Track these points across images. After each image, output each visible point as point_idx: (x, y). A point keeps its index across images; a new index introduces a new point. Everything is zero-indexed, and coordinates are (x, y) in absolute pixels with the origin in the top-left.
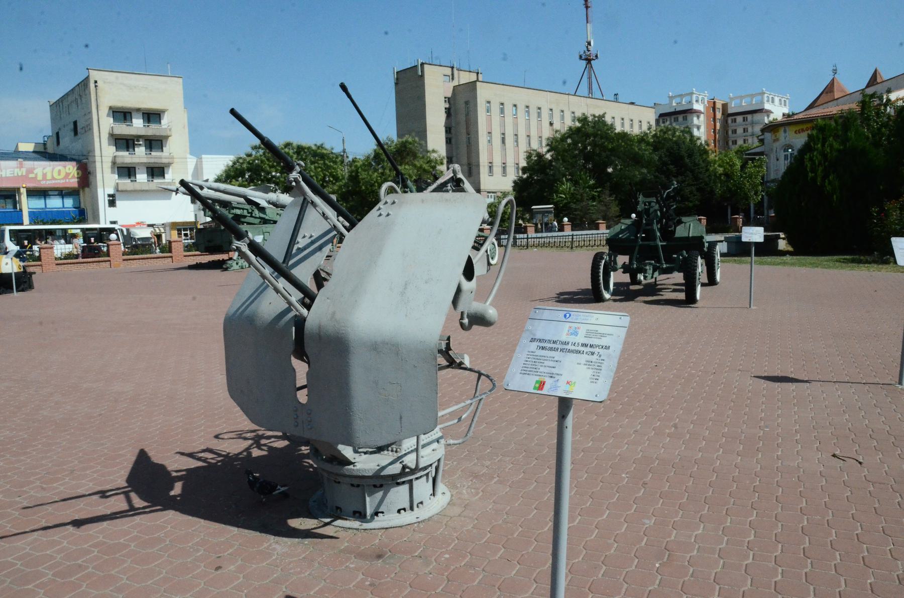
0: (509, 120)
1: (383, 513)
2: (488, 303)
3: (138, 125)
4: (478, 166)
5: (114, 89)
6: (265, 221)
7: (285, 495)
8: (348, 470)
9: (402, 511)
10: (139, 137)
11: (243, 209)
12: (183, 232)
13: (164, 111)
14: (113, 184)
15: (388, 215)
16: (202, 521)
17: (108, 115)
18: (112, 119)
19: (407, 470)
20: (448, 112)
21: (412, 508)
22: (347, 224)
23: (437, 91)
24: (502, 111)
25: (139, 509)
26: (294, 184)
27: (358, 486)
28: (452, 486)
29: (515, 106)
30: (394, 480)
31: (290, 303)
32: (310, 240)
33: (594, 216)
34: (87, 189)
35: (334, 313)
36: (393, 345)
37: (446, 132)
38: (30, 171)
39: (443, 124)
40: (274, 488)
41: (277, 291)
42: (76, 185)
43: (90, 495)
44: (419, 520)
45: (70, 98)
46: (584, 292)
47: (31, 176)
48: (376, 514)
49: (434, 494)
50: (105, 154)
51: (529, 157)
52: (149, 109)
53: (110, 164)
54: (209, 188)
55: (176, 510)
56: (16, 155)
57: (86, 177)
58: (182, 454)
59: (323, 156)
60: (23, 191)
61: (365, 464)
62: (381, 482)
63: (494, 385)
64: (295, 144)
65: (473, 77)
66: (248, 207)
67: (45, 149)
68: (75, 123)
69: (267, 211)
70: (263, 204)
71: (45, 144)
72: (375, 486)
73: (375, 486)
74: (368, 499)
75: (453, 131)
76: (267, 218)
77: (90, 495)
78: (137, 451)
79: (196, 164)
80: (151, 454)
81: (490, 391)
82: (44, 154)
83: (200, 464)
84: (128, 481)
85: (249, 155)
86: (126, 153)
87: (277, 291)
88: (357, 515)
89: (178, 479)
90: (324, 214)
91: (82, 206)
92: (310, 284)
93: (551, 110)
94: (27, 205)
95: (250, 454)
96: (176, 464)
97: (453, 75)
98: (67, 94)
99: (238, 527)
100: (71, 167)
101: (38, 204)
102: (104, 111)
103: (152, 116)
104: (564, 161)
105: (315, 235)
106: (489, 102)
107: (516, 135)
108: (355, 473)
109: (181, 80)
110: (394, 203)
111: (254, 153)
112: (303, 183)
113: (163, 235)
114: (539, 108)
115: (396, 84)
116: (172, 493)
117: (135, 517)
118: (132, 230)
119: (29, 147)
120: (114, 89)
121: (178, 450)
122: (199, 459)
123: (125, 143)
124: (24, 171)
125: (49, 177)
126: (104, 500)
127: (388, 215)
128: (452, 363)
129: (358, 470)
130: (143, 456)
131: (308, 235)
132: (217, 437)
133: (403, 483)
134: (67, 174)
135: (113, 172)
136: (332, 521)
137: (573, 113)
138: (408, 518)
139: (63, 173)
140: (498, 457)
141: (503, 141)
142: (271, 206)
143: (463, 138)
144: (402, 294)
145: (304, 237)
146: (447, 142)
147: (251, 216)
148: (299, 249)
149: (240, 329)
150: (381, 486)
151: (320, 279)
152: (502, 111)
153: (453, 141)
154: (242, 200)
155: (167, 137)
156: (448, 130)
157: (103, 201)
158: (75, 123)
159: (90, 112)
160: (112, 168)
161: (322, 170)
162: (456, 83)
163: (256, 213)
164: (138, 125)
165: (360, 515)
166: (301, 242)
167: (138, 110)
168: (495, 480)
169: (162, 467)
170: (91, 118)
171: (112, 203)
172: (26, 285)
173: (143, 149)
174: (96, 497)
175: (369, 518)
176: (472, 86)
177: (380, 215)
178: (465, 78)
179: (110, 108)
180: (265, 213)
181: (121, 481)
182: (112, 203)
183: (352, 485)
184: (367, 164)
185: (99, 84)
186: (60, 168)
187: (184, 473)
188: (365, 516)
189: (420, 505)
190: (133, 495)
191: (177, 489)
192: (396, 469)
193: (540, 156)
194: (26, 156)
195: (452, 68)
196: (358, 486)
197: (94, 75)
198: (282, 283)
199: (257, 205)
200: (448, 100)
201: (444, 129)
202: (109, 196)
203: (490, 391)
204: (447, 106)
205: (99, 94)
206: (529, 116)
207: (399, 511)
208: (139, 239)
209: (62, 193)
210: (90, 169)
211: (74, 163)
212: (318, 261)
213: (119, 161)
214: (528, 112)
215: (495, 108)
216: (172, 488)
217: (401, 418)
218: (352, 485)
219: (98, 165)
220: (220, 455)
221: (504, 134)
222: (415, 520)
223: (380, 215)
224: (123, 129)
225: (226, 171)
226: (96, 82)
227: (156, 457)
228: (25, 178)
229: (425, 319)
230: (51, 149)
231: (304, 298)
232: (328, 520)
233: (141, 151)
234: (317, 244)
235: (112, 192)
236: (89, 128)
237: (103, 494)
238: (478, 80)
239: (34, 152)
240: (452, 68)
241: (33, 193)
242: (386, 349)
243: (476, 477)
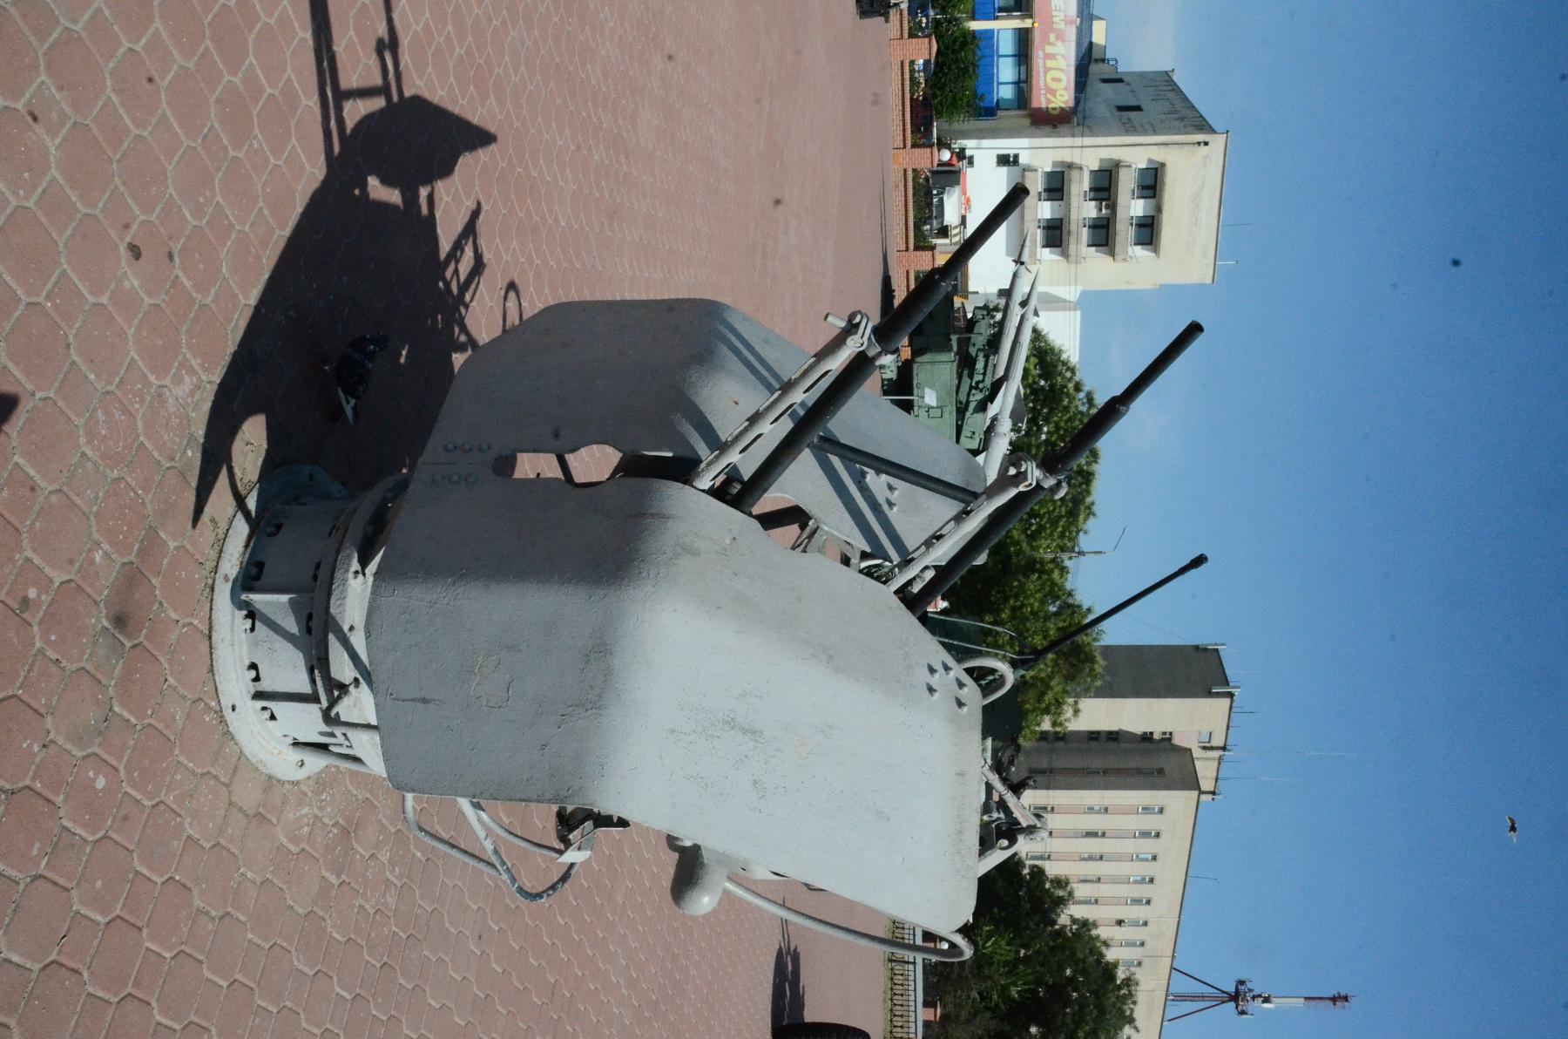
0: (1130, 846)
1: (252, 629)
2: (729, 886)
3: (1134, 208)
4: (1048, 787)
5: (1194, 173)
6: (961, 411)
7: (336, 414)
8: (349, 557)
9: (253, 674)
10: (1113, 207)
13: (1156, 250)
14: (1035, 163)
15: (931, 690)
16: (287, 232)
17: (1150, 161)
18: (1143, 166)
19: (336, 693)
20: (1147, 738)
21: (259, 695)
22: (916, 588)
23: (1181, 718)
24: (1145, 834)
25: (339, 109)
26: (1012, 471)
27: (315, 578)
28: (322, 782)
29: (1154, 858)
30: (318, 663)
31: (721, 447)
32: (881, 501)
33: (949, 999)
34: (1027, 121)
35: (694, 552)
36: (600, 696)
37: (1111, 733)
38: (1061, 36)
39: (1125, 728)
40: (350, 392)
41: (754, 419)
42: (1035, 105)
43: (390, 21)
44: (228, 713)
45: (1179, 105)
46: (798, 1003)
47: (1052, 37)
48: (252, 615)
49: (296, 744)
50: (1087, 153)
51: (1060, 883)
52: (1159, 225)
53: (1069, 160)
54: (1023, 317)
55: (324, 183)
56: (1086, 15)
57: (1048, 121)
58: (476, 214)
59: (1073, 514)
60: (1027, 23)
61: (355, 595)
62: (316, 632)
63: (539, 895)
64: (1095, 467)
65: (1207, 785)
66: (988, 382)
67: (1096, 61)
68: (1138, 108)
69: (979, 416)
70: (993, 409)
71: (1103, 60)
72: (310, 617)
73: (310, 617)
74: (285, 598)
75: (1112, 745)
76: (968, 414)
77: (390, 21)
78: (492, 128)
79: (1065, 301)
80: (483, 154)
81: (520, 890)
82: (1087, 60)
83: (445, 247)
84: (417, 101)
85: (1078, 388)
86: (1086, 186)
87: (754, 419)
88: (254, 571)
89: (411, 199)
90: (939, 538)
91: (1000, 113)
92: (774, 498)
93: (1145, 924)
94: (1004, 29)
95: (461, 348)
96: (449, 202)
97: (1212, 748)
98: (1186, 99)
99: (257, 308)
101: (1006, 45)
102: (1158, 155)
103: (1148, 232)
104: (1052, 949)
105: (893, 514)
106: (1161, 811)
107: (1101, 858)
108: (338, 574)
109: (1208, 280)
110: (960, 704)
111: (1082, 395)
112: (1012, 492)
113: (946, 241)
114: (1148, 902)
115: (1197, 648)
116: (373, 182)
117: (316, 97)
118: (957, 191)
119: (1099, 34)
120: (1194, 173)
121: (485, 207)
122: (458, 246)
123: (1104, 185)
124: (1062, 26)
125: (1050, 63)
126: (373, 44)
127: (931, 690)
128: (568, 822)
129: (345, 582)
130: (481, 138)
131: (895, 496)
132: (512, 286)
133: (313, 681)
134: (1053, 92)
135: (1055, 164)
136: (247, 514)
137: (1139, 964)
138: (234, 686)
139: (1055, 83)
140: (399, 878)
141: (1091, 834)
142: (988, 422)
143: (1097, 763)
144: (731, 724)
145: (891, 488)
146: (1092, 733)
147: (971, 388)
148: (864, 475)
149: (694, 332)
150: (309, 631)
151: (794, 515)
152: (1145, 834)
153: (1093, 744)
154: (1000, 373)
155: (1112, 254)
156: (1114, 736)
157: (1009, 145)
158: (1138, 108)
159: (1155, 133)
160: (1063, 163)
162: (1197, 753)
163: (977, 396)
164: (1134, 208)
165: (252, 578)
166: (877, 482)
167: (1159, 209)
168: (333, 879)
169: (446, 170)
170: (1145, 133)
171: (1004, 160)
172: (866, 7)
173: (1093, 214)
174: (382, 30)
175: (243, 597)
176: (1190, 781)
177: (932, 670)
178: (1206, 770)
179: (1163, 165)
180: (976, 411)
181: (417, 83)
182: (1004, 160)
183: (318, 566)
184: (1053, 591)
185: (1203, 148)
186: (1064, 83)
187: (425, 210)
188: (251, 590)
189: (267, 714)
190: (379, 103)
191: (377, 189)
192: (342, 668)
193: (1061, 902)
194: (1084, 30)
195: (1224, 748)
196: (315, 578)
197: (1217, 142)
198: (773, 432)
199: (991, 398)
200: (1167, 739)
201: (1114, 728)
202: (1016, 157)
203: (520, 890)
204: (1156, 736)
205: (1186, 148)
206: (1136, 882)
207: (253, 666)
208: (941, 200)
209: (1023, 86)
210: (1062, 128)
211: (1071, 104)
212: (835, 523)
213: (1075, 174)
214: (1142, 881)
215: (1150, 822)
216: (386, 181)
217: (425, 701)
218: (318, 566)
219: (1068, 141)
220: (464, 288)
221: (1104, 835)
222: (226, 702)
223: (932, 670)
224: (1127, 182)
225: (1052, 349)
226: (1206, 144)
227: (469, 164)
228: (1049, 26)
229: (654, 778)
230: (1094, 68)
231: (741, 481)
232: (252, 503)
233: (1090, 210)
234: (871, 519)
235: (1022, 160)
236: (1130, 129)
237: (388, 45)
238: (1201, 792)
239: (1091, 43)
240: (1224, 748)
241: (1024, 40)
242: (591, 683)
243: (346, 832)
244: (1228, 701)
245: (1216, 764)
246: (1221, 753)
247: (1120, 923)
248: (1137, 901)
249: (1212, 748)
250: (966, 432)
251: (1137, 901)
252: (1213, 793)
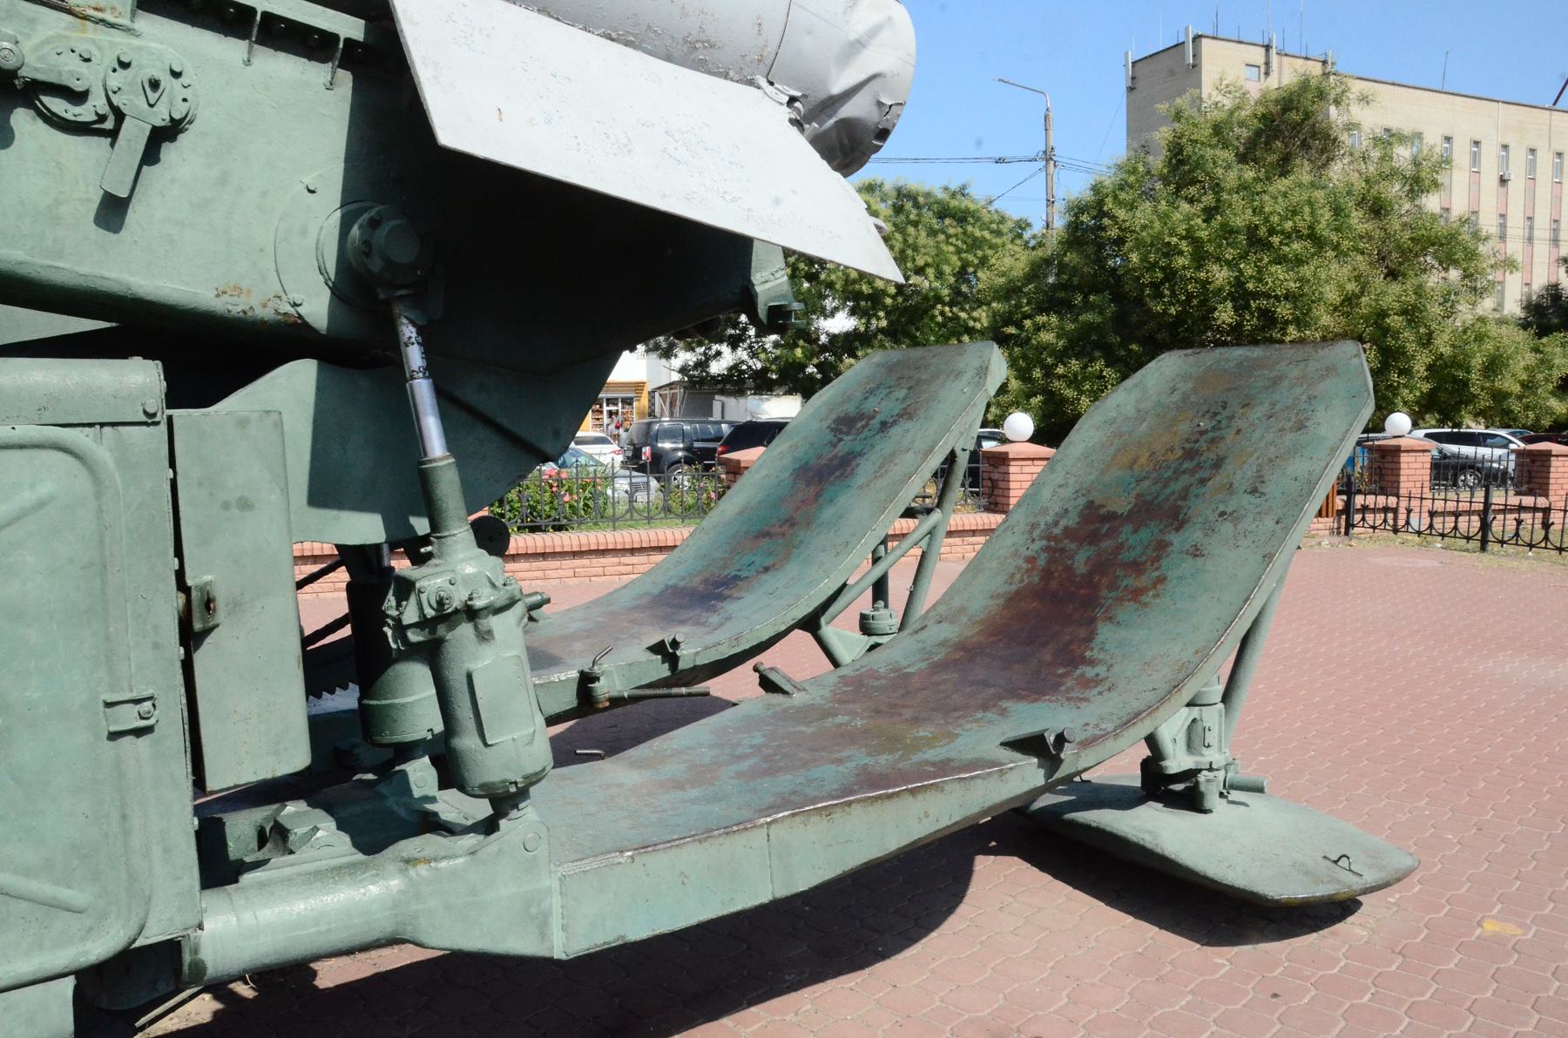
12: (605, 409)
59: (962, 217)
64: (888, 187)
93: (1505, 147)
97: (1267, 64)
114: (1477, 143)
115: (1131, 89)
161: (959, 251)
195: (1268, 48)
240: (1268, 48)
244: (1204, 41)
245: (1285, 59)
246: (1273, 52)
247: (1503, 181)
248: (1475, 159)
249: (1267, 64)
251: (1475, 159)
252: (1324, 63)
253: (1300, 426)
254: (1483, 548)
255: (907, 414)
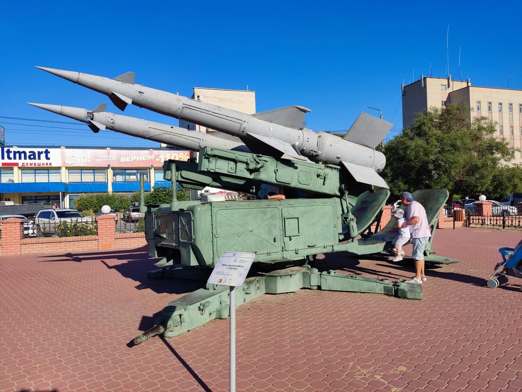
11: (235, 161)
38: (157, 156)
47: (157, 160)
100: (183, 154)
115: (403, 96)
124: (153, 156)
162: (450, 90)
176: (466, 90)
185: (200, 98)
226: (198, 97)
246: (450, 80)
250: (316, 186)
253: (437, 201)
254: (504, 228)
255: (374, 200)
